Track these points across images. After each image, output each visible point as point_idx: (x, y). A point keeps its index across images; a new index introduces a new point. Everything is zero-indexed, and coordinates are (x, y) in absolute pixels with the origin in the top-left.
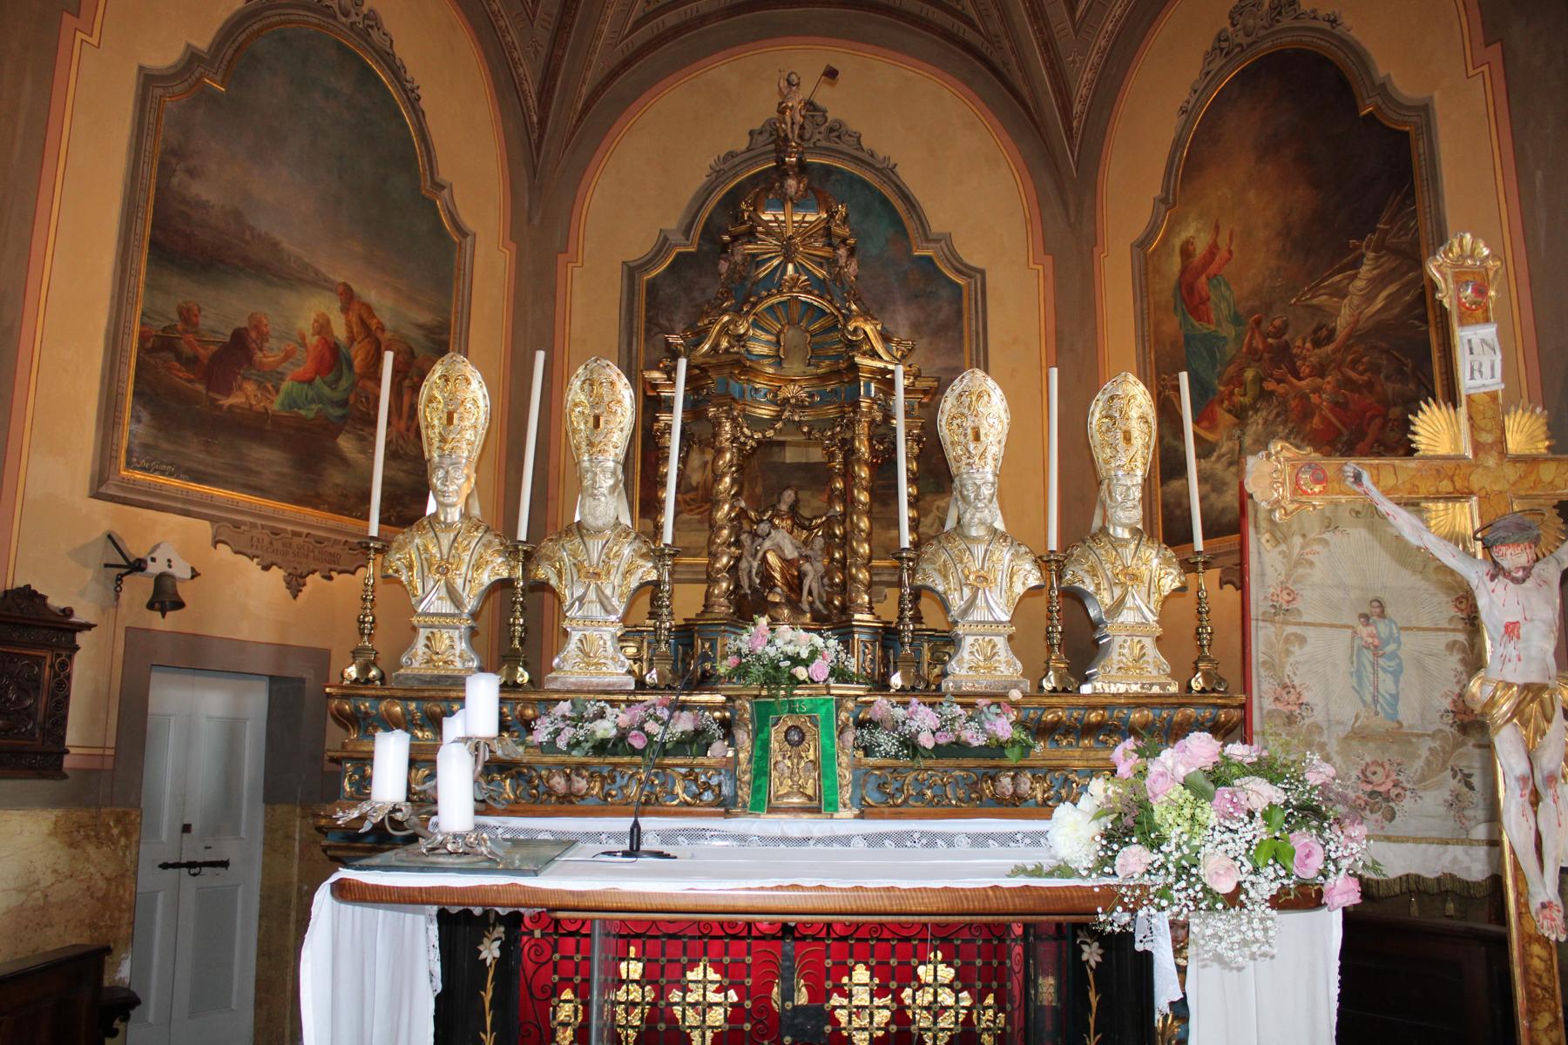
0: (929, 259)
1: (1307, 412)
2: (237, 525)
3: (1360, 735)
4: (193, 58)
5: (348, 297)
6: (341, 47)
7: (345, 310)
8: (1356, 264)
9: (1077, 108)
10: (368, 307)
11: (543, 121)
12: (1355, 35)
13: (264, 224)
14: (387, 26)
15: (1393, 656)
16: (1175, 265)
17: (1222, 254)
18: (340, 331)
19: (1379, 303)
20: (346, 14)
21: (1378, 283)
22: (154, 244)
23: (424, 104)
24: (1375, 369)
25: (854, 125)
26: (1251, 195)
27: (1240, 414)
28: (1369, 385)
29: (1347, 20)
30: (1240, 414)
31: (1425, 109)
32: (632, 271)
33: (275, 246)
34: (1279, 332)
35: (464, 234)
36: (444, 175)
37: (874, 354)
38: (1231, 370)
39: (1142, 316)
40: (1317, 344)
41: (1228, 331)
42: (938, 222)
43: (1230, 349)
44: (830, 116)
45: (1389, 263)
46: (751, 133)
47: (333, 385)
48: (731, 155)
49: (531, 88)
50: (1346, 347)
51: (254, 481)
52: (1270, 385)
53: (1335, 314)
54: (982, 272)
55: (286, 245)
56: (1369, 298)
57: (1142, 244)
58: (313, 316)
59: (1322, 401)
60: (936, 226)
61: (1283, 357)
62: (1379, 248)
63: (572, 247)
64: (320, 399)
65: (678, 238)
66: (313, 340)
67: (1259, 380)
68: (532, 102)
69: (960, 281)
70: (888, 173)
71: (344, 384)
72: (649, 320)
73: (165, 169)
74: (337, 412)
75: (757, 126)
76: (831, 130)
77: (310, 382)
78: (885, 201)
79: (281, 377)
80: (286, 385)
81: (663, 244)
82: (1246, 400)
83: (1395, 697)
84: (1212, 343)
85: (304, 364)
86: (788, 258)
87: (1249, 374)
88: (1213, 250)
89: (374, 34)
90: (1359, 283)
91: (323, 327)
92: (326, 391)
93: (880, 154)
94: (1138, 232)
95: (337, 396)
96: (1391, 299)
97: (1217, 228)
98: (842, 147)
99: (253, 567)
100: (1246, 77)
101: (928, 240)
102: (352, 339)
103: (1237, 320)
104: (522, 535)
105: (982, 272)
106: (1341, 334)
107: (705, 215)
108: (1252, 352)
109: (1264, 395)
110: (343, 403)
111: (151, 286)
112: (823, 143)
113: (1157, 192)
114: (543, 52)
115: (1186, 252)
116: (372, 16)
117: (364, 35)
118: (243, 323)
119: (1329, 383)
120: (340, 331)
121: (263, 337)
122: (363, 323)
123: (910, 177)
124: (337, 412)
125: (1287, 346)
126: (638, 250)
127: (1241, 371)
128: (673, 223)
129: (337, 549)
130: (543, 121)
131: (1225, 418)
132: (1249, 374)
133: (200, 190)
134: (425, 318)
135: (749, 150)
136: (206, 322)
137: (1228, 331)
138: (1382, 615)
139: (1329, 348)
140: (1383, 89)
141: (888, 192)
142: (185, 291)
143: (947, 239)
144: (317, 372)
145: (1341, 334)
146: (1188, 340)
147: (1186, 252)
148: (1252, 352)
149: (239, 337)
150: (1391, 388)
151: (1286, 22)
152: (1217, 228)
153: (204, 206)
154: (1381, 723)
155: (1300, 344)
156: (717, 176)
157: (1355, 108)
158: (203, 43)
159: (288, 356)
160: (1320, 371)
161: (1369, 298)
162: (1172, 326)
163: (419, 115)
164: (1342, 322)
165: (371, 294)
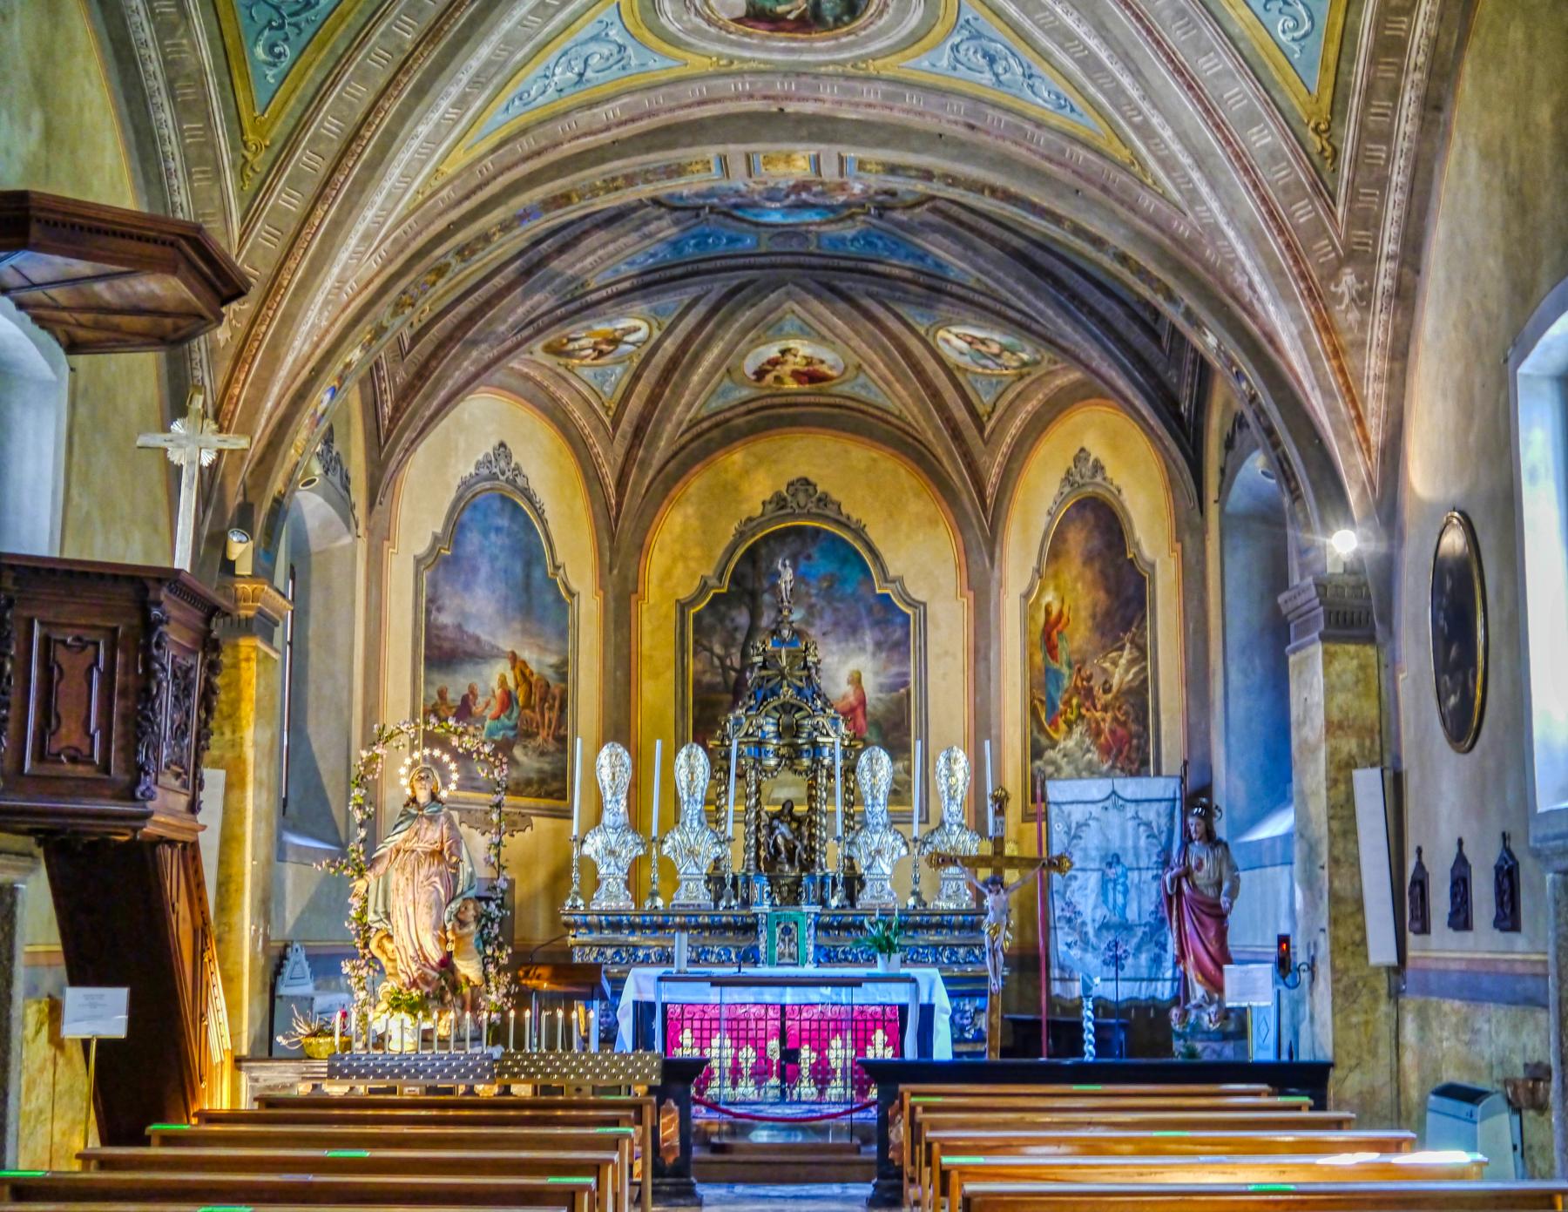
0: (887, 596)
1: (1098, 733)
2: (469, 811)
3: (1105, 926)
4: (436, 539)
5: (514, 658)
6: (504, 498)
7: (513, 668)
8: (1122, 648)
9: (989, 490)
10: (524, 663)
11: (619, 504)
12: (1128, 505)
13: (471, 628)
14: (525, 471)
15: (1124, 884)
16: (1041, 618)
17: (1064, 620)
18: (511, 684)
19: (1130, 676)
20: (503, 473)
21: (1132, 662)
22: (426, 658)
23: (546, 515)
24: (1126, 714)
25: (836, 496)
26: (1079, 586)
27: (1070, 725)
28: (1124, 724)
29: (1124, 492)
30: (1070, 725)
31: (1153, 566)
32: (683, 607)
33: (478, 640)
34: (1089, 679)
35: (571, 594)
36: (560, 560)
37: (828, 735)
38: (1066, 696)
39: (1024, 647)
40: (1107, 691)
41: (1065, 670)
42: (896, 564)
43: (1066, 683)
44: (819, 489)
45: (1136, 654)
46: (764, 503)
47: (509, 718)
48: (750, 519)
49: (610, 481)
50: (1116, 698)
51: (476, 784)
52: (1083, 711)
53: (1112, 676)
54: (925, 605)
55: (484, 637)
56: (1127, 671)
57: (1026, 596)
58: (497, 677)
59: (1106, 727)
60: (892, 572)
61: (1089, 694)
62: (1132, 642)
63: (640, 588)
64: (506, 728)
65: (713, 582)
66: (498, 692)
67: (1079, 706)
68: (612, 491)
69: (909, 611)
70: (859, 533)
71: (515, 714)
72: (696, 642)
73: (428, 612)
74: (511, 734)
75: (768, 497)
76: (820, 500)
77: (498, 718)
78: (857, 553)
79: (484, 718)
80: (488, 723)
81: (704, 587)
82: (1073, 717)
83: (1125, 906)
84: (1057, 675)
85: (495, 706)
86: (784, 677)
87: (1075, 701)
88: (1061, 614)
89: (519, 480)
90: (1123, 661)
91: (503, 682)
92: (506, 722)
93: (854, 517)
94: (1024, 588)
95: (511, 723)
96: (1136, 675)
97: (1063, 601)
98: (828, 512)
99: (476, 834)
100: (1081, 505)
101: (886, 580)
102: (517, 686)
103: (1070, 666)
104: (654, 833)
105: (925, 605)
106: (1115, 689)
107: (732, 566)
108: (1076, 687)
109: (1081, 717)
110: (515, 727)
111: (428, 682)
112: (814, 510)
113: (1034, 564)
114: (620, 460)
115: (1048, 613)
116: (517, 468)
117: (513, 482)
118: (466, 691)
119: (1109, 716)
120: (511, 684)
121: (475, 696)
122: (523, 674)
123: (873, 534)
124: (511, 734)
125: (1090, 690)
126: (684, 594)
127: (1070, 699)
128: (709, 572)
129: (516, 818)
130: (619, 504)
131: (1063, 727)
132: (1075, 701)
133: (445, 619)
134: (553, 659)
135: (762, 515)
136: (450, 696)
137: (1065, 670)
138: (1118, 862)
139: (1109, 696)
140: (1137, 545)
141: (858, 546)
142: (441, 680)
143: (899, 580)
144: (502, 710)
145: (1115, 689)
146: (1047, 670)
147: (1048, 613)
148: (1076, 687)
149: (465, 699)
150: (1134, 728)
151: (1099, 479)
152: (1063, 601)
153: (445, 627)
154: (1116, 919)
155: (1098, 691)
156: (741, 536)
157: (1124, 552)
158: (439, 530)
159: (487, 704)
160: (1105, 709)
161: (1127, 671)
162: (1039, 658)
163: (544, 522)
164: (1115, 682)
165: (526, 654)
